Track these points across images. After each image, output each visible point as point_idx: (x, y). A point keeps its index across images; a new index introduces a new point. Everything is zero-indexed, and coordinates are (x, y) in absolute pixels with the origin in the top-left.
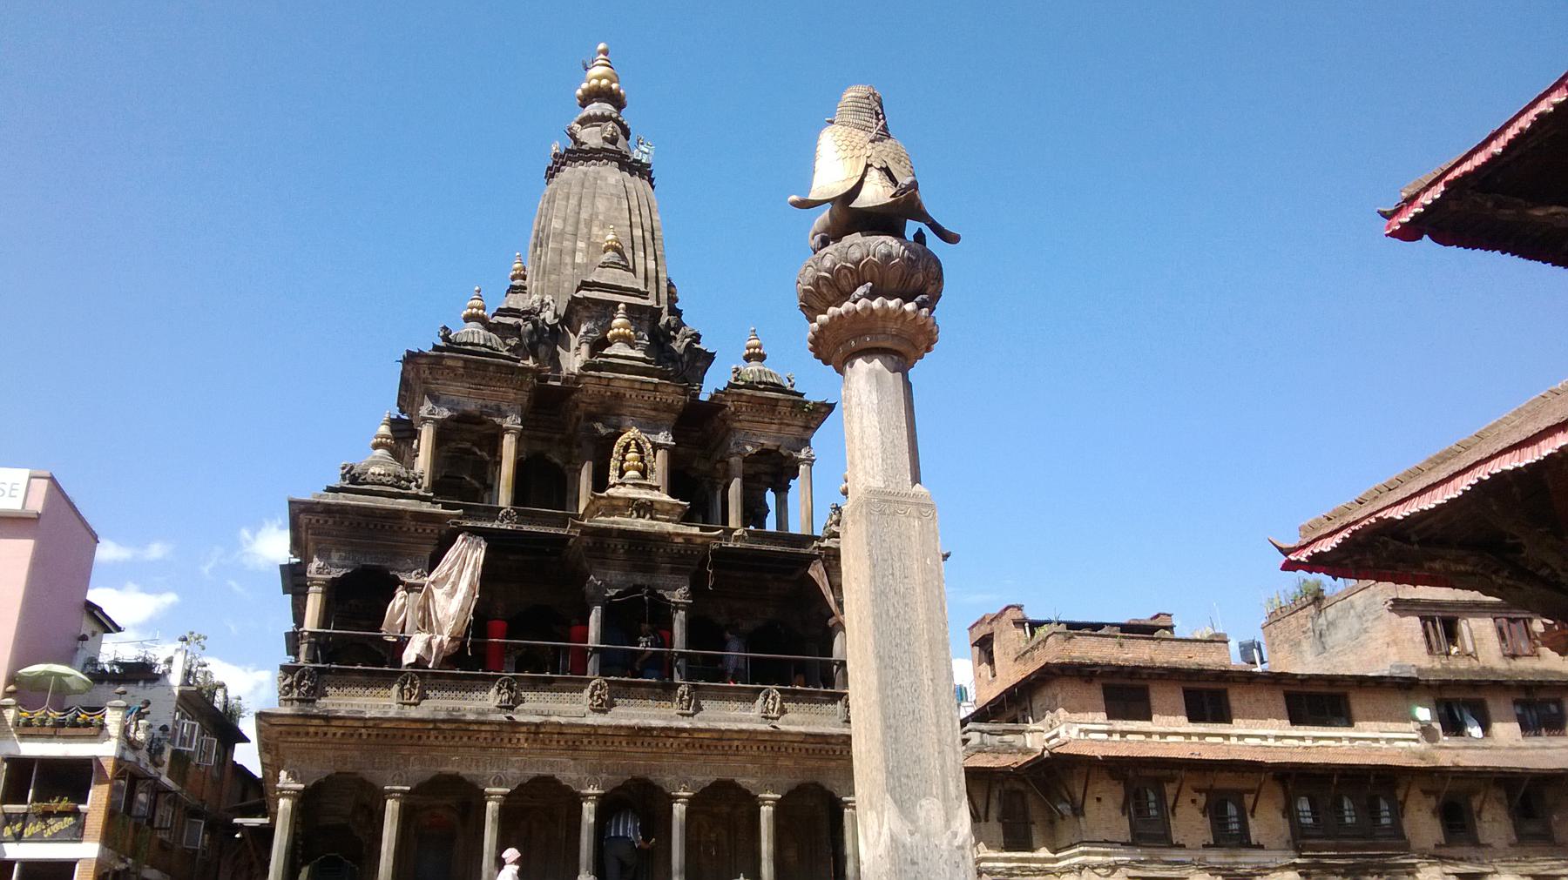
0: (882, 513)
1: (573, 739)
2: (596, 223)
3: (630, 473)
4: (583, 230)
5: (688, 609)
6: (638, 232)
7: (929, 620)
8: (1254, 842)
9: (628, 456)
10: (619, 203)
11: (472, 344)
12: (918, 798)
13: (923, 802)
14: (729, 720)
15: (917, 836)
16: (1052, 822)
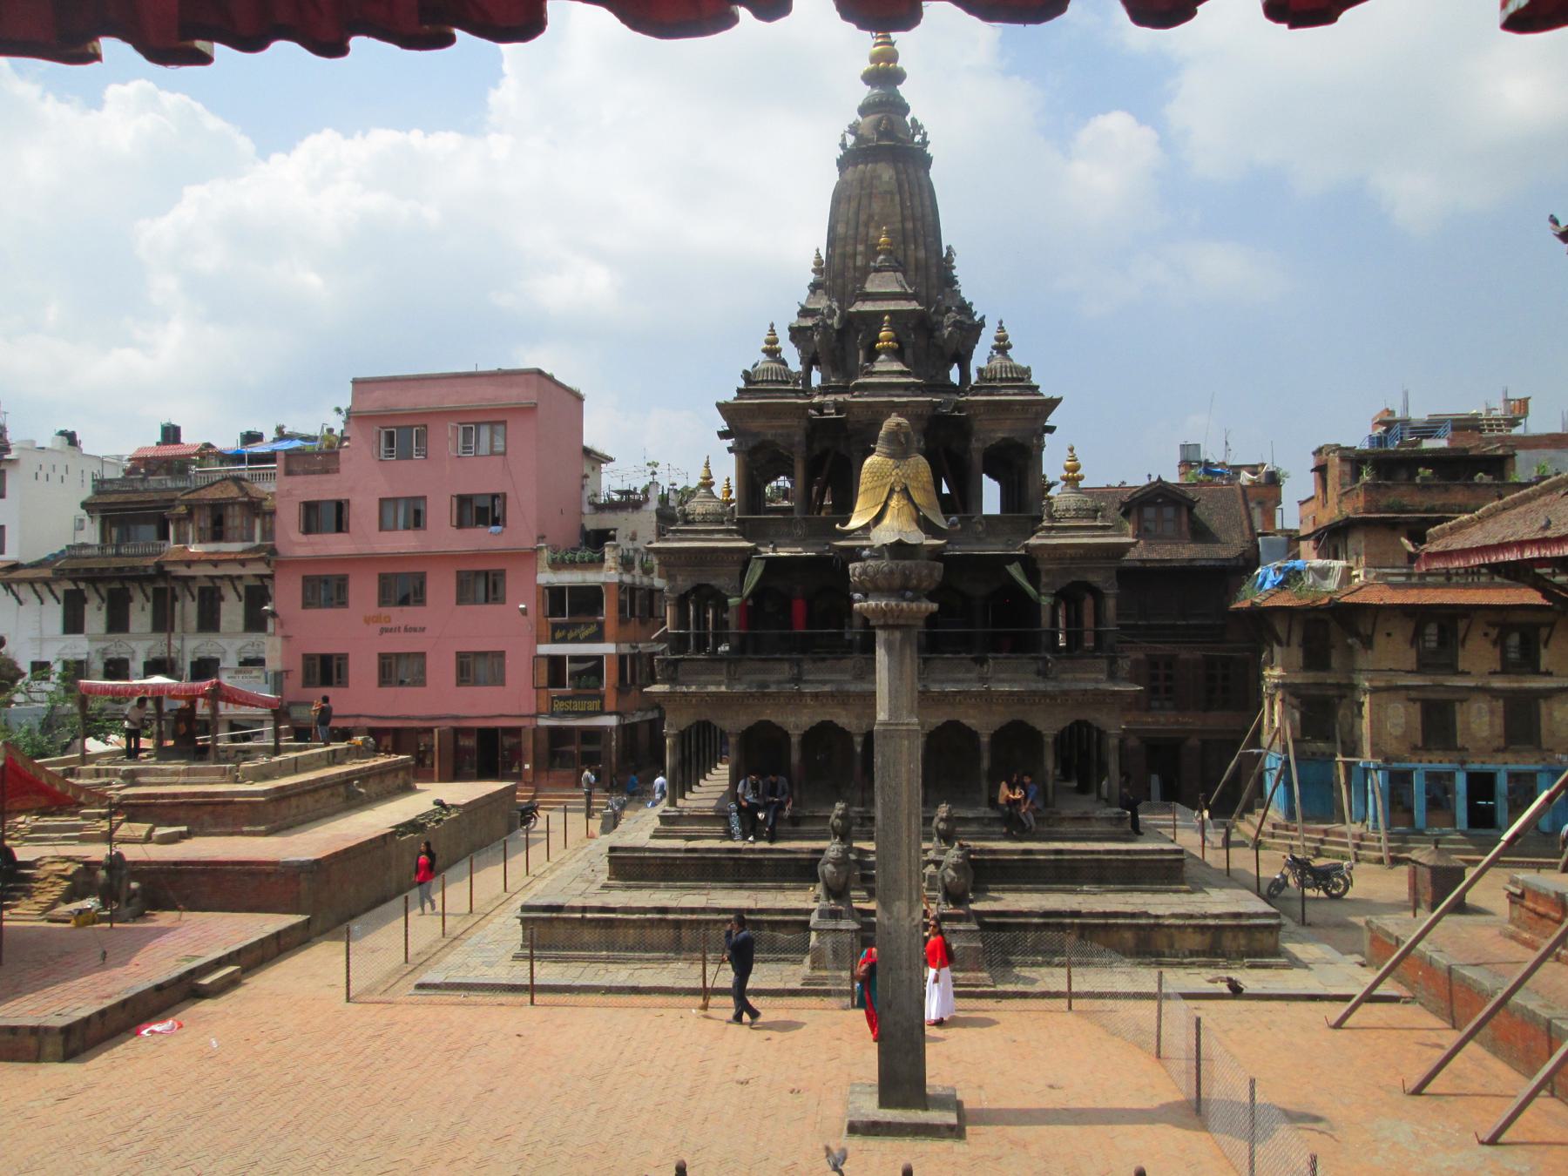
6: (909, 225)
8: (1543, 668)
10: (892, 200)
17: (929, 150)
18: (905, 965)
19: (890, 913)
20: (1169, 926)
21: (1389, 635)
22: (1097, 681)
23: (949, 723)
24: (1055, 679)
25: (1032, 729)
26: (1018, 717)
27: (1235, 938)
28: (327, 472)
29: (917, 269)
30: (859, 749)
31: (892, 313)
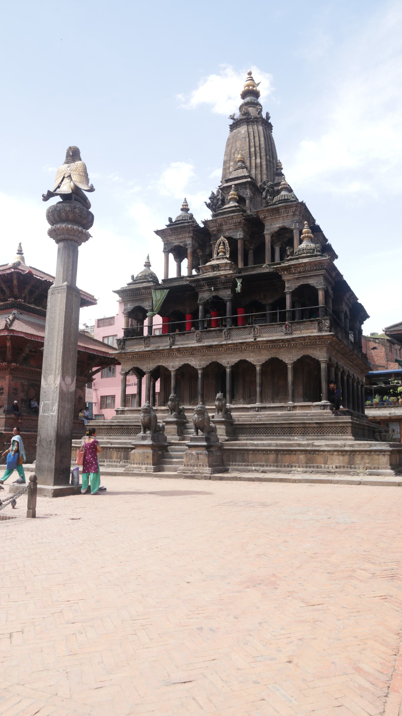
1: (192, 351)
2: (237, 152)
3: (220, 254)
6: (253, 149)
7: (59, 324)
9: (220, 247)
12: (49, 375)
13: (50, 376)
17: (269, 121)
19: (47, 382)
20: (324, 451)
22: (312, 333)
23: (241, 360)
24: (291, 334)
25: (282, 361)
26: (273, 356)
27: (362, 458)
28: (111, 325)
29: (256, 167)
30: (200, 376)
31: (235, 185)
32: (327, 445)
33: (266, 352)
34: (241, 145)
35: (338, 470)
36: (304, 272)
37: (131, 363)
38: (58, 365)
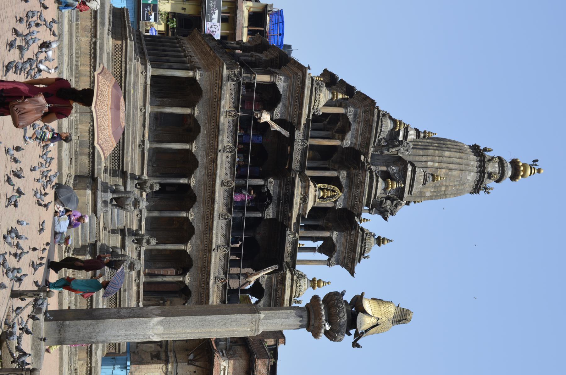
0: (252, 319)
1: (212, 175)
4: (444, 165)
5: (261, 219)
10: (457, 181)
11: (382, 125)
12: (163, 326)
14: (217, 233)
15: (152, 326)
16: (187, 350)
18: (127, 333)
21: (195, 372)
23: (193, 228)
26: (194, 264)
30: (182, 181)
31: (404, 187)
32: (96, 361)
33: (200, 256)
34: (454, 176)
35: (73, 371)
36: (276, 295)
37: (209, 87)
38: (174, 336)
